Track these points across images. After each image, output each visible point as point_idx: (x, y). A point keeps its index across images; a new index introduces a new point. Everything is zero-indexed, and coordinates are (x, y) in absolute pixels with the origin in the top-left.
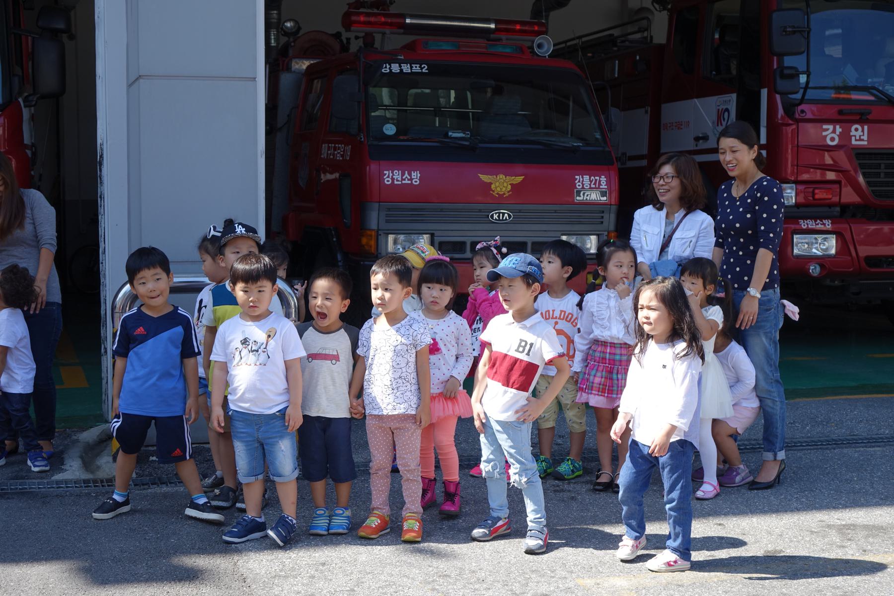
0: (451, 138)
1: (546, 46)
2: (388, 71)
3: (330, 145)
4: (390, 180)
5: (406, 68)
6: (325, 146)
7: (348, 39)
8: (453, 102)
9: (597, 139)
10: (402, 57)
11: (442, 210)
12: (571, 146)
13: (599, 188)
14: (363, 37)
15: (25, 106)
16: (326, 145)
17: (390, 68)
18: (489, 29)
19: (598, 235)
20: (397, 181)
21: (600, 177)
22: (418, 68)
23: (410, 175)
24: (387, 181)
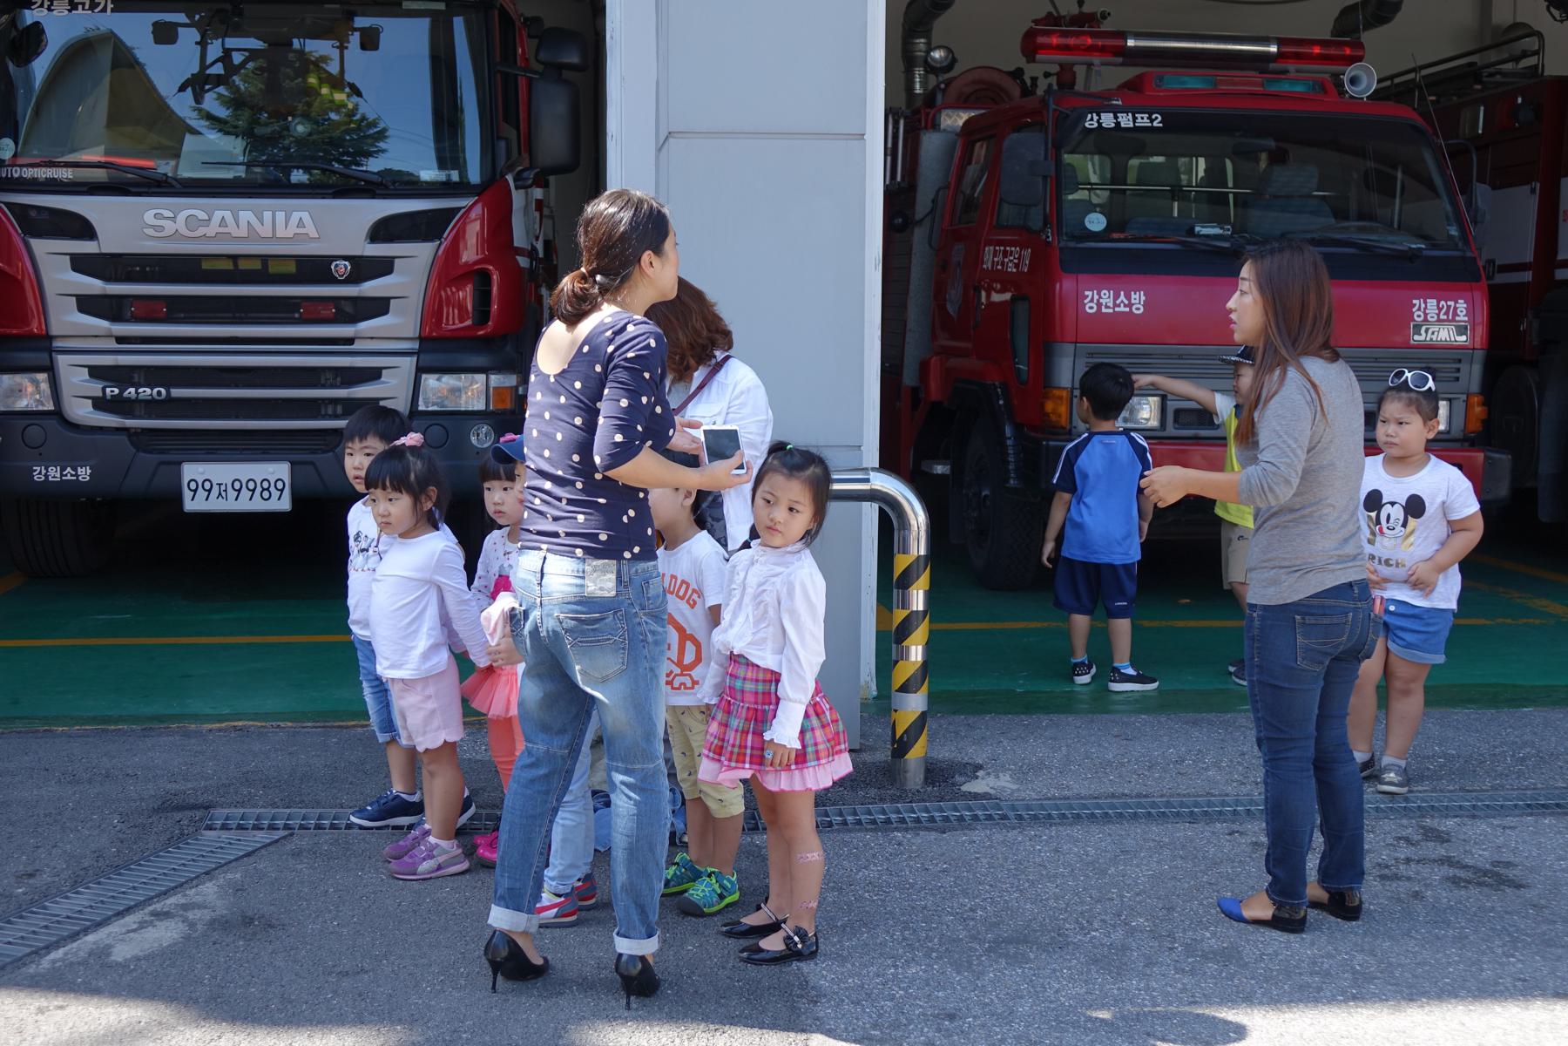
0: (1199, 236)
1: (1364, 80)
2: (1096, 125)
3: (997, 248)
4: (1095, 307)
5: (1126, 121)
6: (989, 249)
7: (1034, 80)
8: (1202, 178)
9: (1451, 237)
10: (1120, 103)
11: (1180, 357)
12: (1405, 248)
13: (1454, 320)
14: (1057, 74)
15: (517, 188)
16: (992, 248)
17: (1098, 121)
18: (1268, 54)
19: (1450, 400)
20: (1107, 307)
21: (1456, 302)
22: (1146, 120)
23: (1128, 297)
24: (1091, 307)
